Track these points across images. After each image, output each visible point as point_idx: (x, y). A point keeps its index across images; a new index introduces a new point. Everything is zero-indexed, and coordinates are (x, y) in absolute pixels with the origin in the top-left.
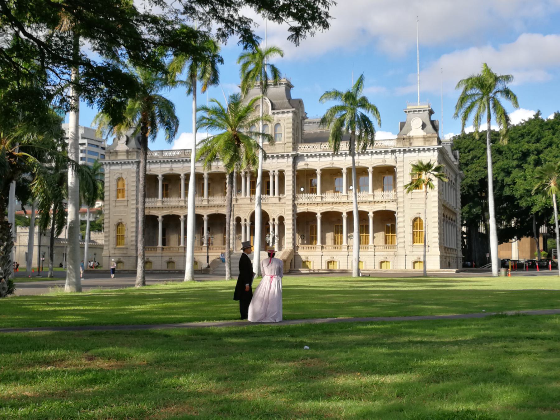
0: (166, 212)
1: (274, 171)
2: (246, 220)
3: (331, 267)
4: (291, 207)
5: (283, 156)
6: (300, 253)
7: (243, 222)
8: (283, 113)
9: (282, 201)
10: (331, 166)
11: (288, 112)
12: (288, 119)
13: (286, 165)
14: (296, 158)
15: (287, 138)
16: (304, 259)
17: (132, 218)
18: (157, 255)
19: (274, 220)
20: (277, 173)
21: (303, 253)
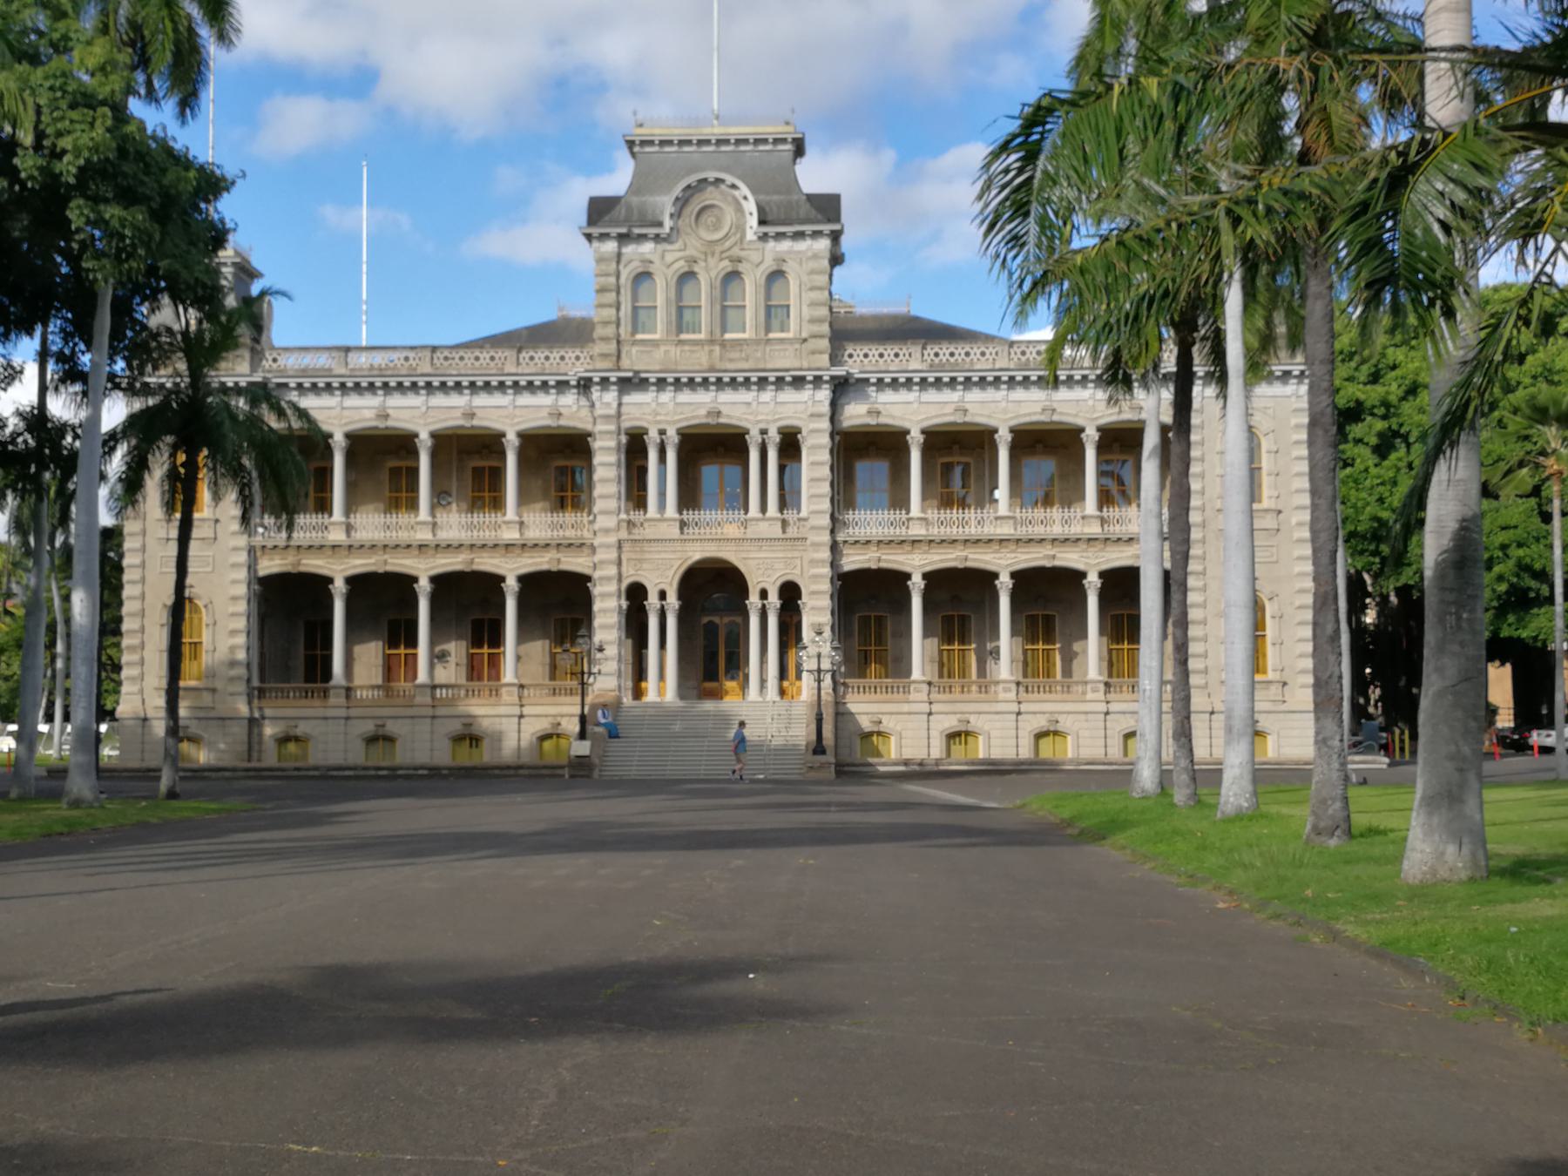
0: (361, 564)
1: (764, 432)
2: (663, 595)
3: (1047, 750)
4: (826, 554)
5: (798, 382)
6: (853, 707)
7: (653, 601)
8: (799, 235)
9: (792, 532)
10: (959, 418)
11: (816, 234)
12: (815, 256)
13: (807, 410)
14: (842, 388)
15: (812, 321)
16: (866, 724)
17: (234, 582)
18: (331, 713)
19: (764, 594)
20: (774, 437)
21: (865, 707)
